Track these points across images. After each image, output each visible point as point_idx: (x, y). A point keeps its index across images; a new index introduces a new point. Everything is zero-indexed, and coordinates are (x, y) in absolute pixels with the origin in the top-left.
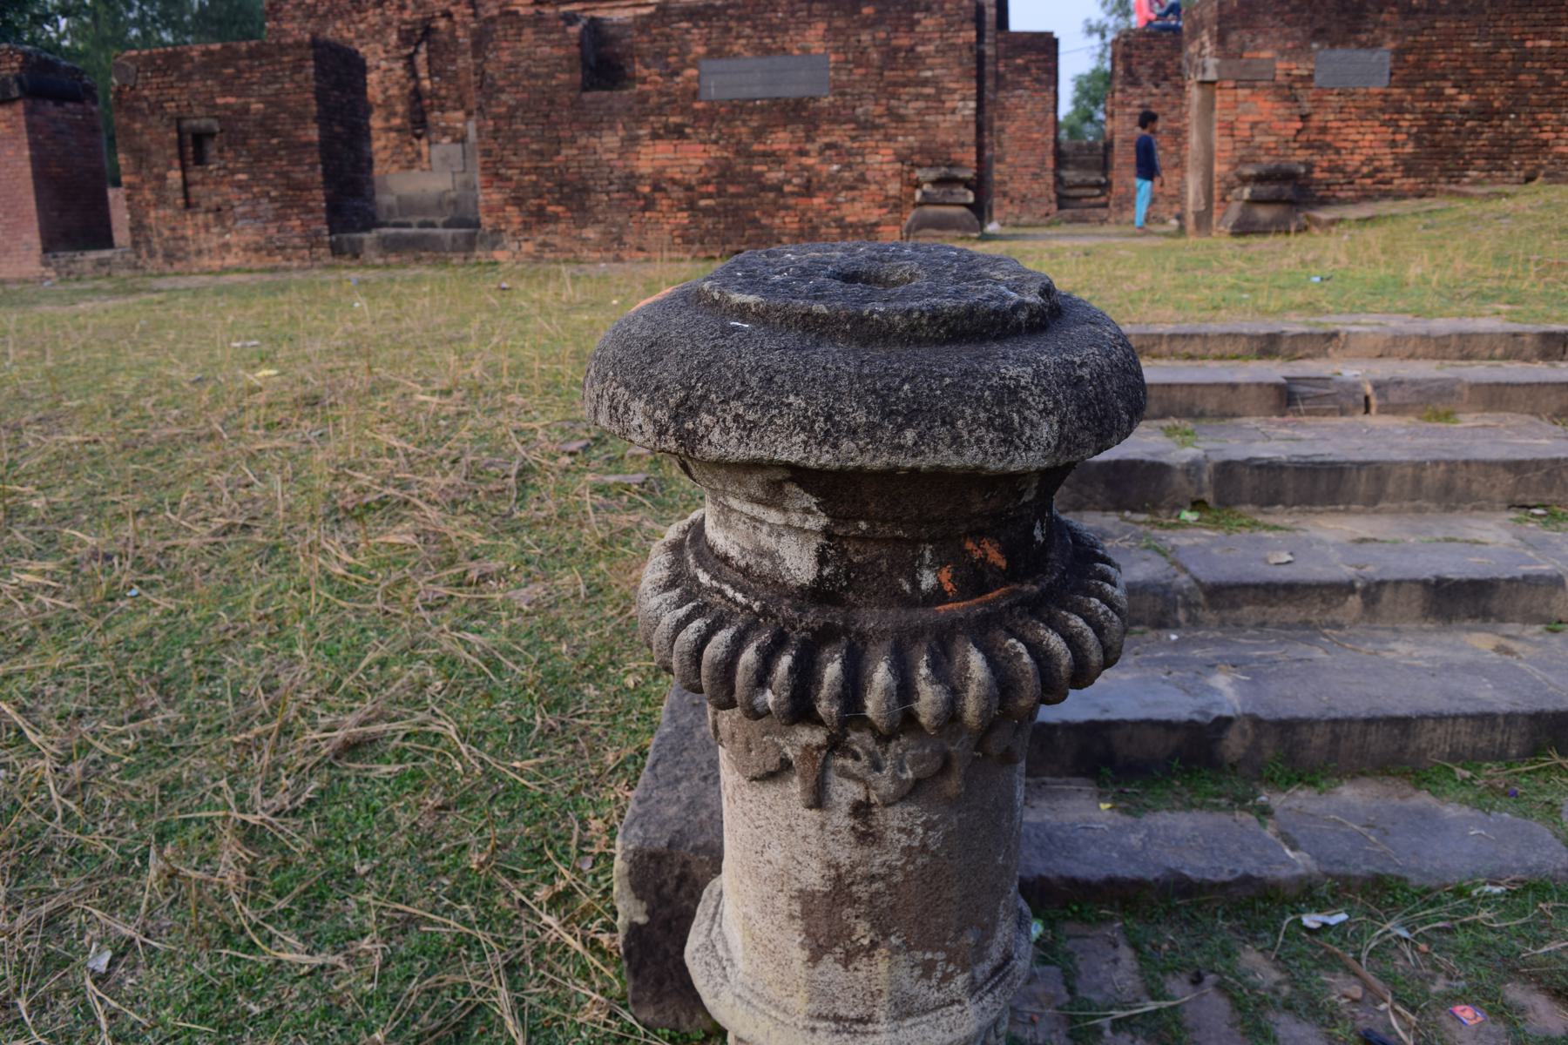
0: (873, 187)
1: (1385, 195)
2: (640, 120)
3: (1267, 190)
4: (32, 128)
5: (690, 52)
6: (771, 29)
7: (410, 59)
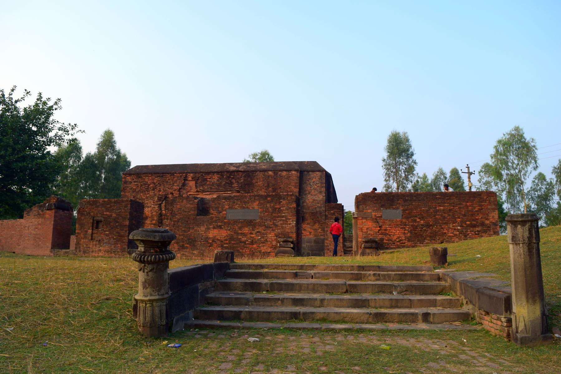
0: (269, 243)
1: (404, 247)
2: (210, 224)
3: (368, 245)
4: (55, 216)
5: (224, 207)
6: (245, 202)
7: (160, 204)
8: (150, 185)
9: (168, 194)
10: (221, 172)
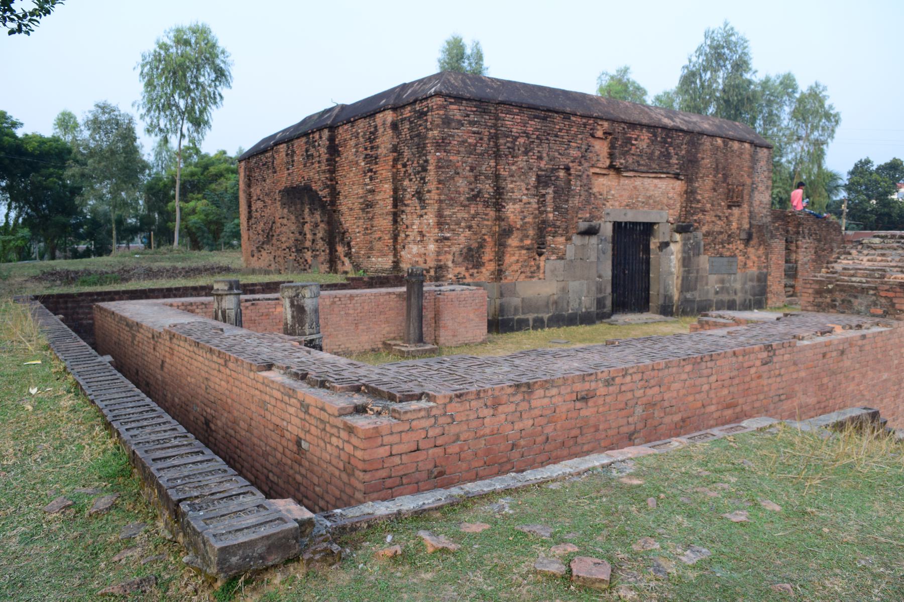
8: (518, 137)
9: (559, 168)
10: (655, 127)
